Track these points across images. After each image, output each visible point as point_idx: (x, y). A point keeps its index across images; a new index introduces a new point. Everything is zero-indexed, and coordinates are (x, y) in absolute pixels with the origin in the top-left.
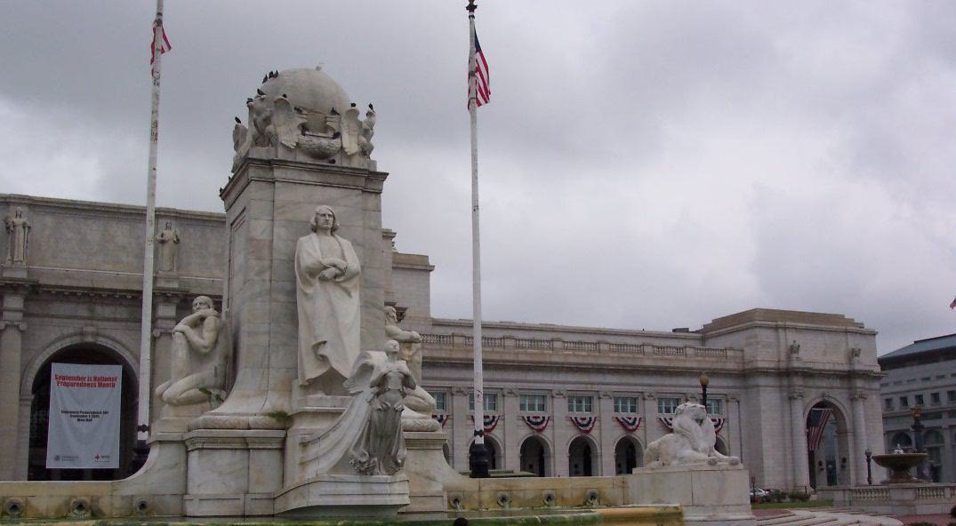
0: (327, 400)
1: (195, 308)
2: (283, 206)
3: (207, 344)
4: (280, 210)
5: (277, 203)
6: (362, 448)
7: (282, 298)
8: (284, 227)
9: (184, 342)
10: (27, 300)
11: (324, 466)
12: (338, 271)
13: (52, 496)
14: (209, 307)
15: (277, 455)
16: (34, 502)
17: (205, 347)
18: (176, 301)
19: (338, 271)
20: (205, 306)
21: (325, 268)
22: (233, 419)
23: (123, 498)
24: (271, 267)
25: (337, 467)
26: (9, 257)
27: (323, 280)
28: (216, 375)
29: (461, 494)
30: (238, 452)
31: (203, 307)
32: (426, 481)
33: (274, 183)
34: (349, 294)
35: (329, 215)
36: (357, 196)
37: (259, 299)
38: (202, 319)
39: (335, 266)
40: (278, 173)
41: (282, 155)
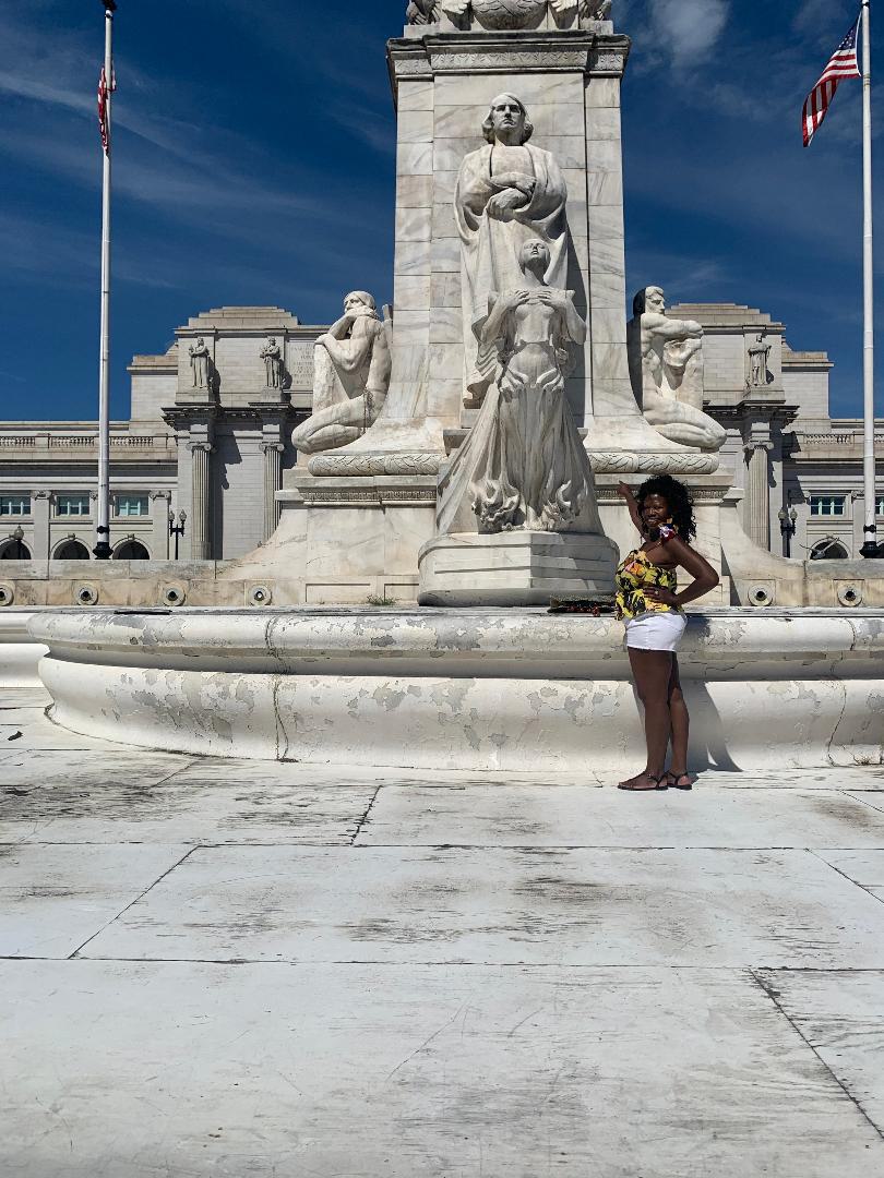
2: (451, 114)
3: (351, 357)
8: (451, 148)
12: (518, 194)
17: (350, 362)
19: (518, 194)
21: (496, 189)
22: (362, 462)
24: (431, 218)
27: (497, 214)
35: (513, 108)
36: (576, 82)
38: (351, 322)
39: (512, 185)
41: (446, 26)
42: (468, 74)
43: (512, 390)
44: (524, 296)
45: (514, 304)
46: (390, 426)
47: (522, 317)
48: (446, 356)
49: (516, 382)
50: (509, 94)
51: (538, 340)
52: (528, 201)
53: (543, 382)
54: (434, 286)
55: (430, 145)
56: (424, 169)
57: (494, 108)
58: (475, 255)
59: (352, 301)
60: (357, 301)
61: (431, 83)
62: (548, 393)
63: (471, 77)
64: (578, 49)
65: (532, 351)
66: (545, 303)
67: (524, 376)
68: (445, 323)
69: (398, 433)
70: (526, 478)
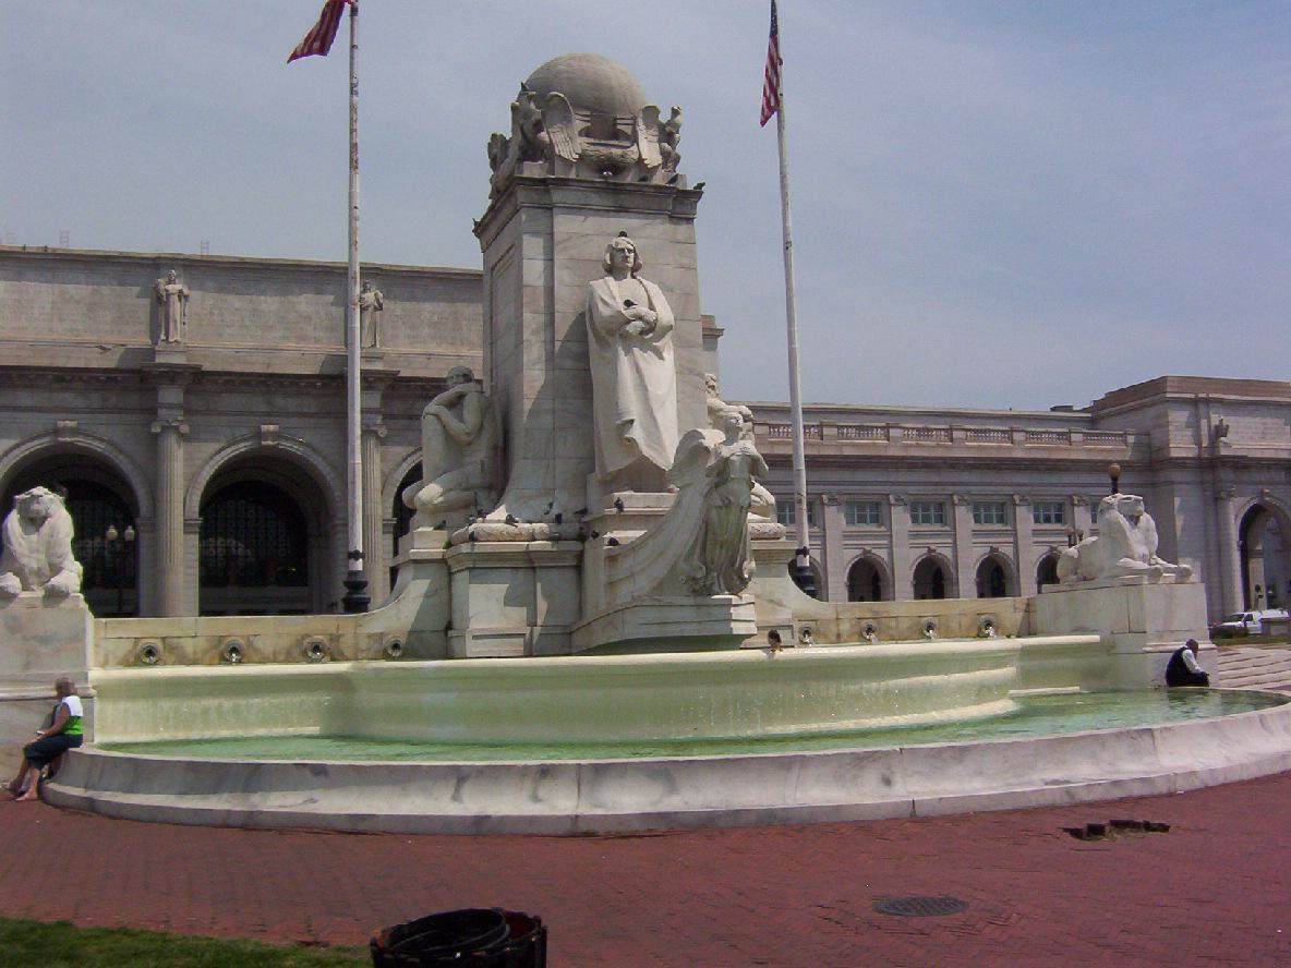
0: (638, 498)
4: (561, 246)
5: (557, 237)
6: (696, 562)
7: (568, 363)
8: (567, 267)
10: (187, 392)
11: (643, 584)
13: (279, 635)
15: (570, 575)
16: (259, 643)
17: (468, 434)
18: (382, 386)
23: (370, 636)
25: (659, 587)
26: (163, 337)
29: (812, 624)
30: (521, 572)
32: (771, 605)
33: (551, 209)
34: (661, 358)
38: (461, 396)
40: (557, 196)
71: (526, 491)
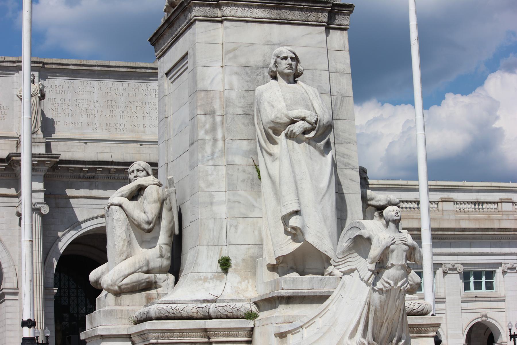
1: (131, 176)
2: (234, 50)
3: (150, 219)
8: (236, 73)
9: (123, 216)
14: (148, 175)
17: (149, 223)
20: (144, 173)
22: (190, 309)
27: (290, 136)
28: (161, 256)
31: (140, 174)
35: (292, 58)
36: (321, 33)
37: (211, 163)
39: (303, 119)
42: (247, 21)
43: (384, 289)
44: (393, 240)
45: (389, 245)
46: (200, 279)
47: (392, 251)
48: (241, 227)
49: (387, 285)
50: (292, 49)
51: (400, 263)
52: (313, 129)
53: (402, 285)
54: (229, 176)
55: (221, 69)
56: (217, 86)
57: (278, 57)
58: (277, 163)
59: (138, 170)
60: (142, 171)
61: (220, 24)
62: (403, 291)
63: (249, 24)
64: (322, 11)
65: (397, 270)
66: (405, 244)
67: (392, 283)
68: (239, 202)
69: (207, 285)
70: (380, 335)
71: (201, 274)
